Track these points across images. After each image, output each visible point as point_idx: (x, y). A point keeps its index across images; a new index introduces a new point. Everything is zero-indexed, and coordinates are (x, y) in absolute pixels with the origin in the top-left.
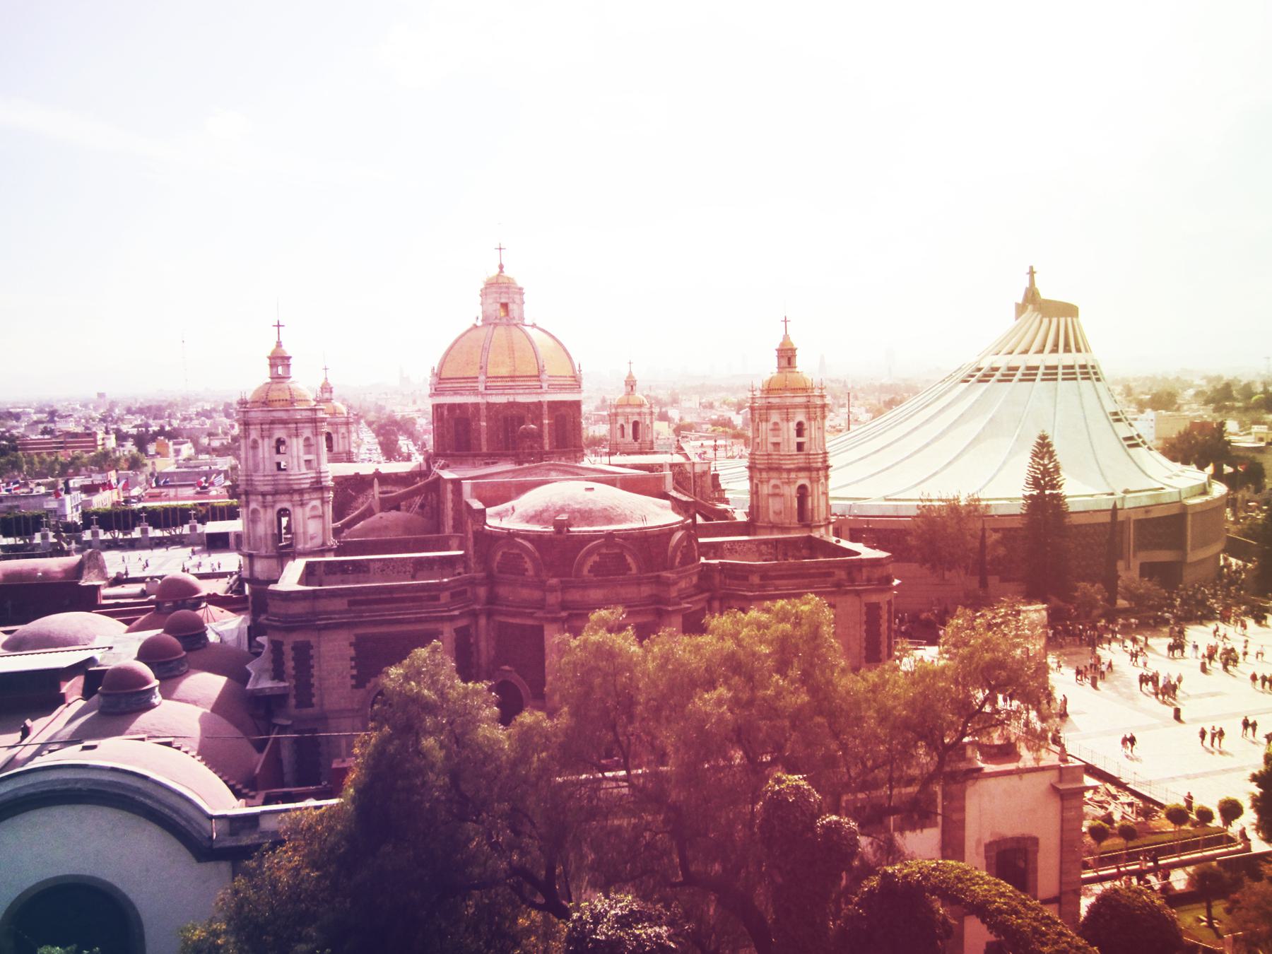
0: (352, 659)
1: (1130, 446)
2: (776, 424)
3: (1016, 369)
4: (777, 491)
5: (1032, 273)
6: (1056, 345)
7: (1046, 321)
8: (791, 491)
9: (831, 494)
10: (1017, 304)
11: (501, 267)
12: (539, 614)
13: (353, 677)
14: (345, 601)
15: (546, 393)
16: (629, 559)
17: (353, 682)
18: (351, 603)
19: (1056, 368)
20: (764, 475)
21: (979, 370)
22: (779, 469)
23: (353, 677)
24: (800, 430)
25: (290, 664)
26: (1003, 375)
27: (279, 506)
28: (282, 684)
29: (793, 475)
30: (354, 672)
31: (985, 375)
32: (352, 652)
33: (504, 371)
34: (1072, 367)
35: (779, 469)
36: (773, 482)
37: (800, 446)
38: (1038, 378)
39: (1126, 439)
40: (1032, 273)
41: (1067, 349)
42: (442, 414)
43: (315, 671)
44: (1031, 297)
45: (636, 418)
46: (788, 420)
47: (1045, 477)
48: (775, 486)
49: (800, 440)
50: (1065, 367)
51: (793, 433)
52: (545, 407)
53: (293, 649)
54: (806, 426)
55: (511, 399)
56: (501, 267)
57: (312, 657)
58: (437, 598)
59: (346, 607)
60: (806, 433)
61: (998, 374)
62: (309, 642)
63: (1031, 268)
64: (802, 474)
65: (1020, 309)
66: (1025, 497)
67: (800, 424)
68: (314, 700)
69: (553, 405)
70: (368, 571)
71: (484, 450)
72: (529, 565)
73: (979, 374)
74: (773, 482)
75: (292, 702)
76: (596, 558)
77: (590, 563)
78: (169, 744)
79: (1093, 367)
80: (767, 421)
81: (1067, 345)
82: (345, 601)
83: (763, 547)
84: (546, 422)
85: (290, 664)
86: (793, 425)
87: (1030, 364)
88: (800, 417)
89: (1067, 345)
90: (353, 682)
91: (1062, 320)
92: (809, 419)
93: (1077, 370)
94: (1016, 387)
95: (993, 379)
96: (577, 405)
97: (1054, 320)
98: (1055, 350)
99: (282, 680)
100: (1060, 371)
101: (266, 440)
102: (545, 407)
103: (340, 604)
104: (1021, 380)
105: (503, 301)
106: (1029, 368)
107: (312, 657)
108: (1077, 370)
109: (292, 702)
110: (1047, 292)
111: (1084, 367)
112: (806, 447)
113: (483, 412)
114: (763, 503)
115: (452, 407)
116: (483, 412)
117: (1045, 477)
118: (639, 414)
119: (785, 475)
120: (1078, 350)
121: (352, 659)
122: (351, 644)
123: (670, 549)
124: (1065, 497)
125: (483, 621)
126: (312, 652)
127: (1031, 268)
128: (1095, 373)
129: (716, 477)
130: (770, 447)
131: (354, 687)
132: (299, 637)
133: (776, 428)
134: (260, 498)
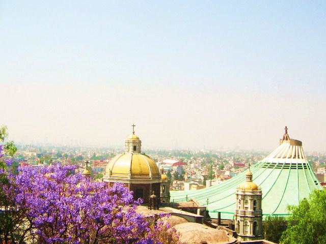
3: (282, 164)
6: (295, 156)
21: (269, 163)
26: (278, 166)
31: (271, 166)
34: (301, 164)
36: (245, 221)
40: (286, 127)
44: (286, 138)
63: (286, 127)
73: (269, 165)
81: (298, 156)
89: (298, 156)
93: (302, 165)
95: (274, 167)
97: (294, 146)
100: (297, 167)
108: (302, 165)
110: (293, 136)
111: (304, 164)
129: (208, 212)
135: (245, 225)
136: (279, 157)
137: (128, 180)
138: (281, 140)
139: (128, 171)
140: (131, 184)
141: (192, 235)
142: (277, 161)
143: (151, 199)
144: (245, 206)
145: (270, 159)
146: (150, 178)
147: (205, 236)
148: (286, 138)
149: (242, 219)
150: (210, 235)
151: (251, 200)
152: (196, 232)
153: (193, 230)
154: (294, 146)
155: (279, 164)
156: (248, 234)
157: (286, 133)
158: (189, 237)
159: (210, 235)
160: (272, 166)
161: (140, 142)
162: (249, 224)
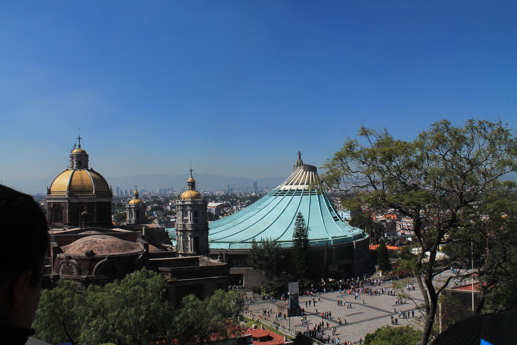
3: (294, 190)
7: (305, 172)
9: (209, 240)
10: (295, 166)
11: (80, 146)
21: (280, 191)
42: (50, 206)
47: (301, 233)
49: (196, 218)
66: (294, 241)
69: (98, 203)
84: (95, 210)
87: (299, 189)
96: (109, 204)
97: (308, 172)
105: (79, 160)
117: (301, 233)
124: (309, 240)
135: (185, 242)
137: (65, 199)
138: (295, 166)
139: (65, 189)
140: (70, 204)
141: (81, 246)
142: (288, 188)
143: (81, 216)
144: (185, 218)
145: (283, 188)
146: (93, 196)
147: (97, 245)
148: (300, 164)
149: (182, 233)
150: (103, 245)
151: (191, 211)
152: (88, 242)
154: (308, 172)
156: (190, 251)
157: (300, 158)
158: (77, 248)
159: (103, 245)
160: (283, 193)
161: (87, 156)
162: (189, 239)
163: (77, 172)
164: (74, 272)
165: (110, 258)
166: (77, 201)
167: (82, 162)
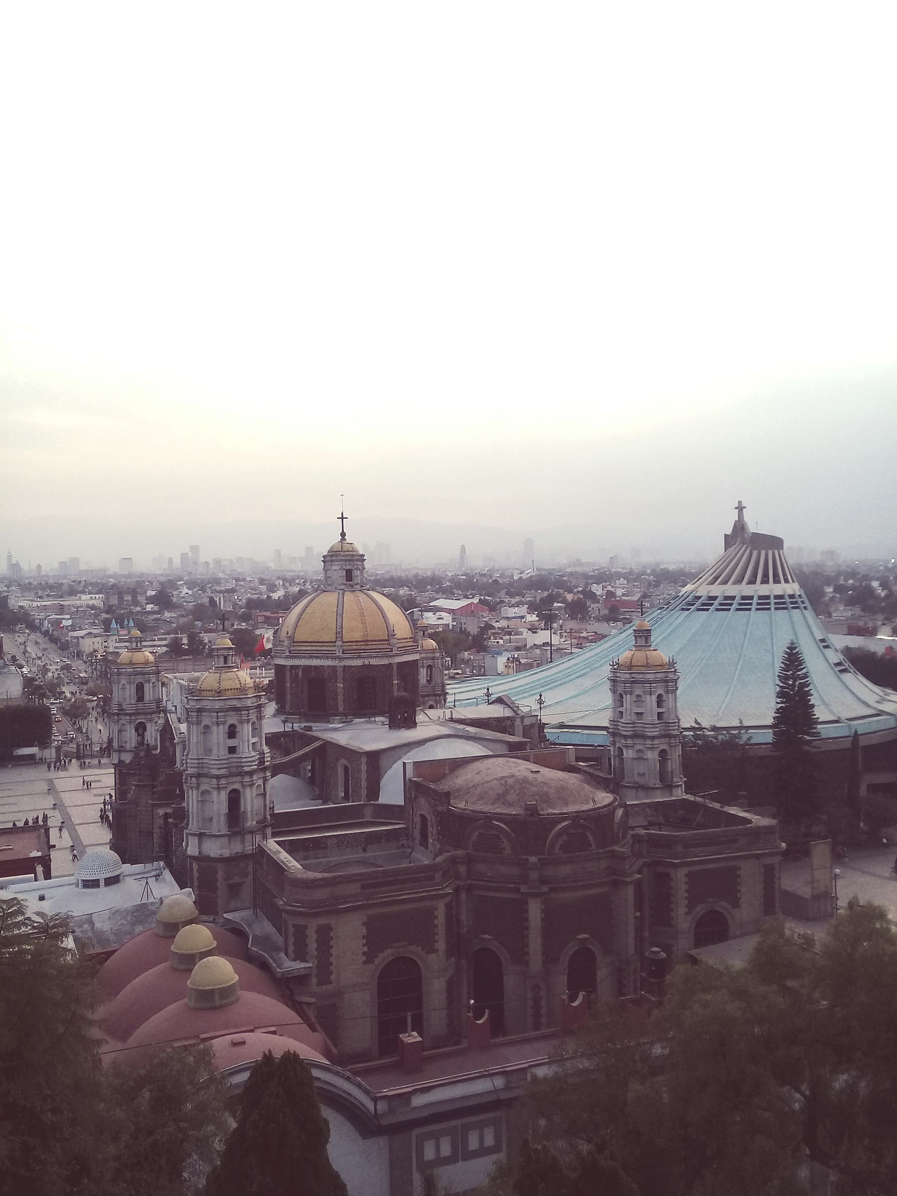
0: (364, 937)
1: (841, 671)
2: (638, 696)
3: (733, 598)
4: (641, 755)
5: (740, 508)
7: (755, 553)
8: (652, 756)
11: (343, 535)
12: (524, 889)
13: (364, 953)
14: (358, 885)
15: (397, 655)
16: (590, 837)
17: (364, 958)
18: (364, 887)
19: (768, 597)
20: (629, 741)
22: (644, 737)
23: (364, 953)
24: (660, 702)
25: (312, 946)
26: (721, 604)
27: (230, 788)
28: (303, 965)
29: (656, 742)
30: (366, 949)
31: (703, 604)
32: (364, 931)
33: (357, 636)
35: (644, 737)
37: (660, 715)
38: (754, 606)
39: (837, 665)
40: (740, 508)
41: (777, 581)
42: (297, 674)
43: (333, 951)
44: (740, 527)
45: (430, 662)
46: (651, 694)
48: (639, 751)
50: (776, 597)
51: (655, 705)
52: (395, 668)
53: (316, 931)
54: (664, 698)
55: (366, 662)
56: (343, 535)
57: (332, 938)
58: (432, 878)
59: (359, 890)
60: (665, 704)
61: (716, 602)
62: (329, 924)
64: (663, 740)
65: (729, 541)
67: (660, 696)
68: (333, 977)
70: (325, 848)
71: (341, 709)
72: (506, 844)
74: (638, 747)
75: (314, 980)
76: (565, 838)
77: (560, 842)
78: (274, 1033)
79: (800, 596)
80: (631, 693)
81: (776, 575)
82: (358, 885)
83: (648, 811)
85: (312, 946)
86: (654, 698)
88: (660, 691)
89: (776, 575)
90: (364, 958)
91: (770, 553)
92: (667, 692)
94: (733, 617)
98: (765, 581)
99: (304, 960)
100: (773, 601)
101: (221, 727)
102: (395, 668)
103: (355, 888)
104: (738, 610)
106: (743, 598)
107: (332, 938)
109: (314, 980)
110: (756, 524)
111: (792, 596)
112: (664, 715)
113: (340, 674)
114: (627, 766)
115: (307, 669)
116: (340, 674)
118: (433, 659)
119: (649, 742)
120: (786, 581)
121: (364, 937)
122: (364, 924)
123: (616, 826)
125: (463, 896)
126: (332, 934)
127: (740, 502)
128: (803, 602)
130: (634, 718)
131: (365, 963)
132: (322, 921)
133: (639, 700)
134: (214, 781)
136: (725, 582)
153: (502, 778)
155: (726, 598)
159: (546, 789)
163: (349, 597)
164: (504, 849)
165: (576, 817)
166: (359, 662)
167: (357, 573)
